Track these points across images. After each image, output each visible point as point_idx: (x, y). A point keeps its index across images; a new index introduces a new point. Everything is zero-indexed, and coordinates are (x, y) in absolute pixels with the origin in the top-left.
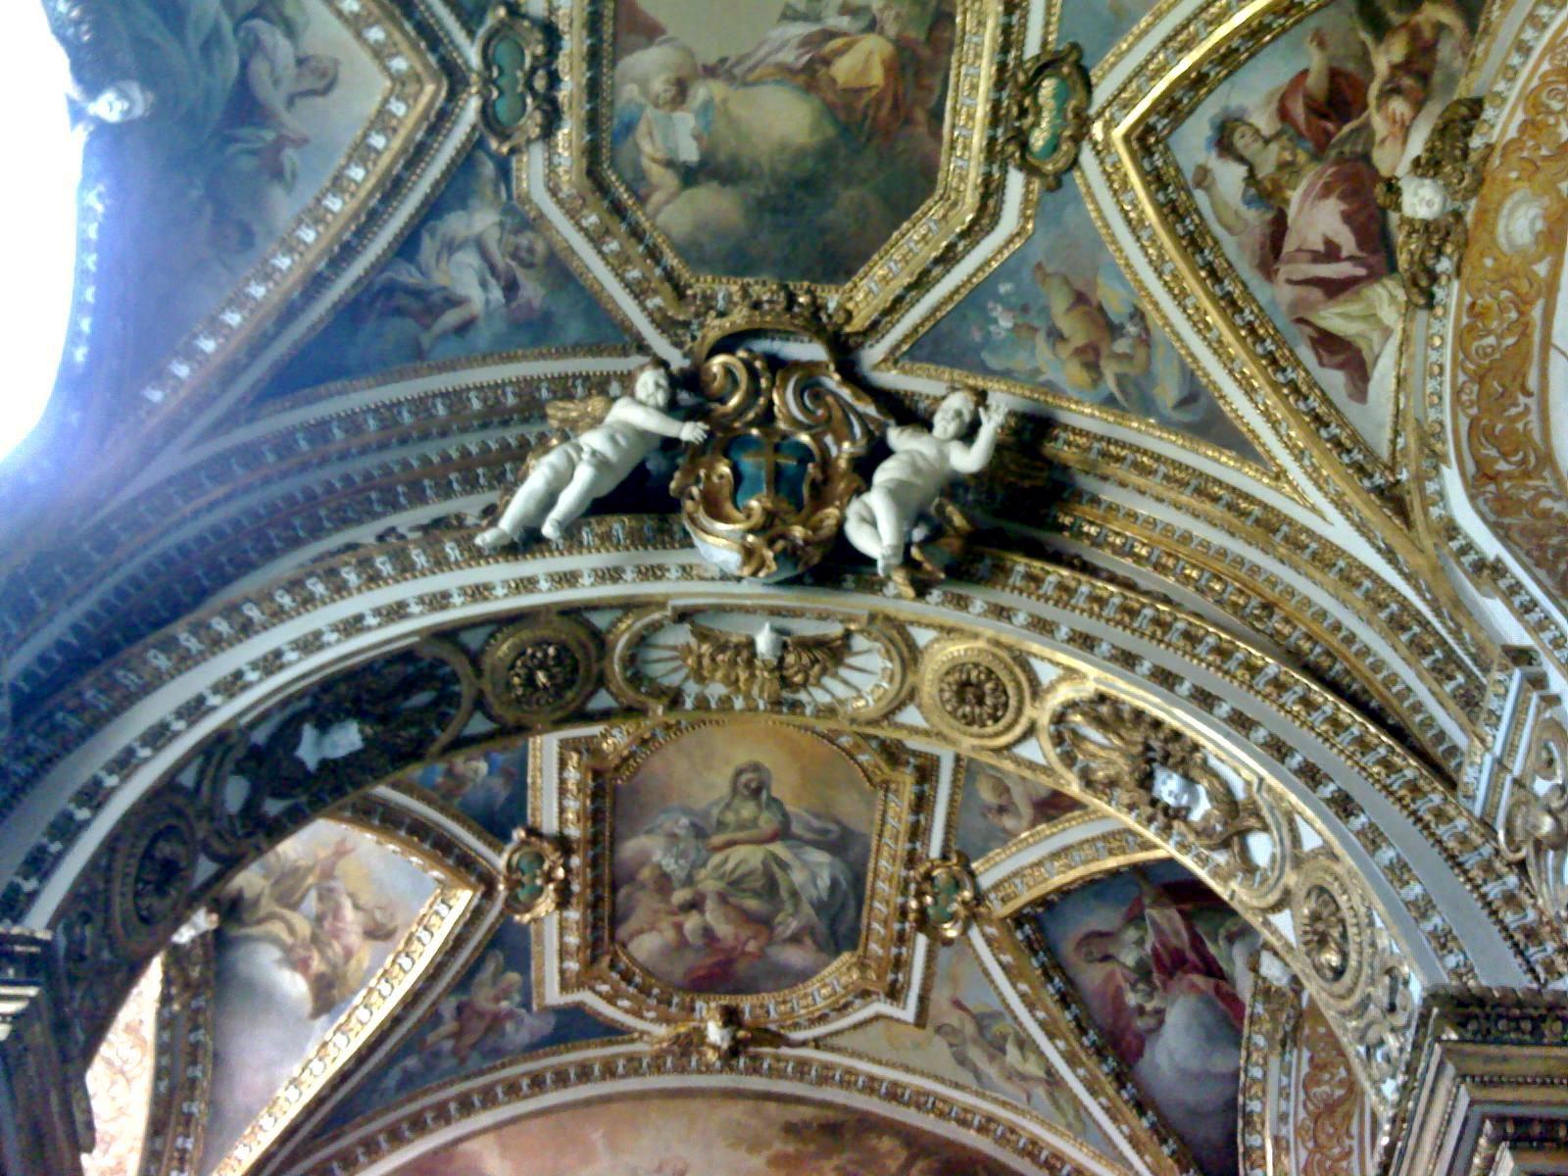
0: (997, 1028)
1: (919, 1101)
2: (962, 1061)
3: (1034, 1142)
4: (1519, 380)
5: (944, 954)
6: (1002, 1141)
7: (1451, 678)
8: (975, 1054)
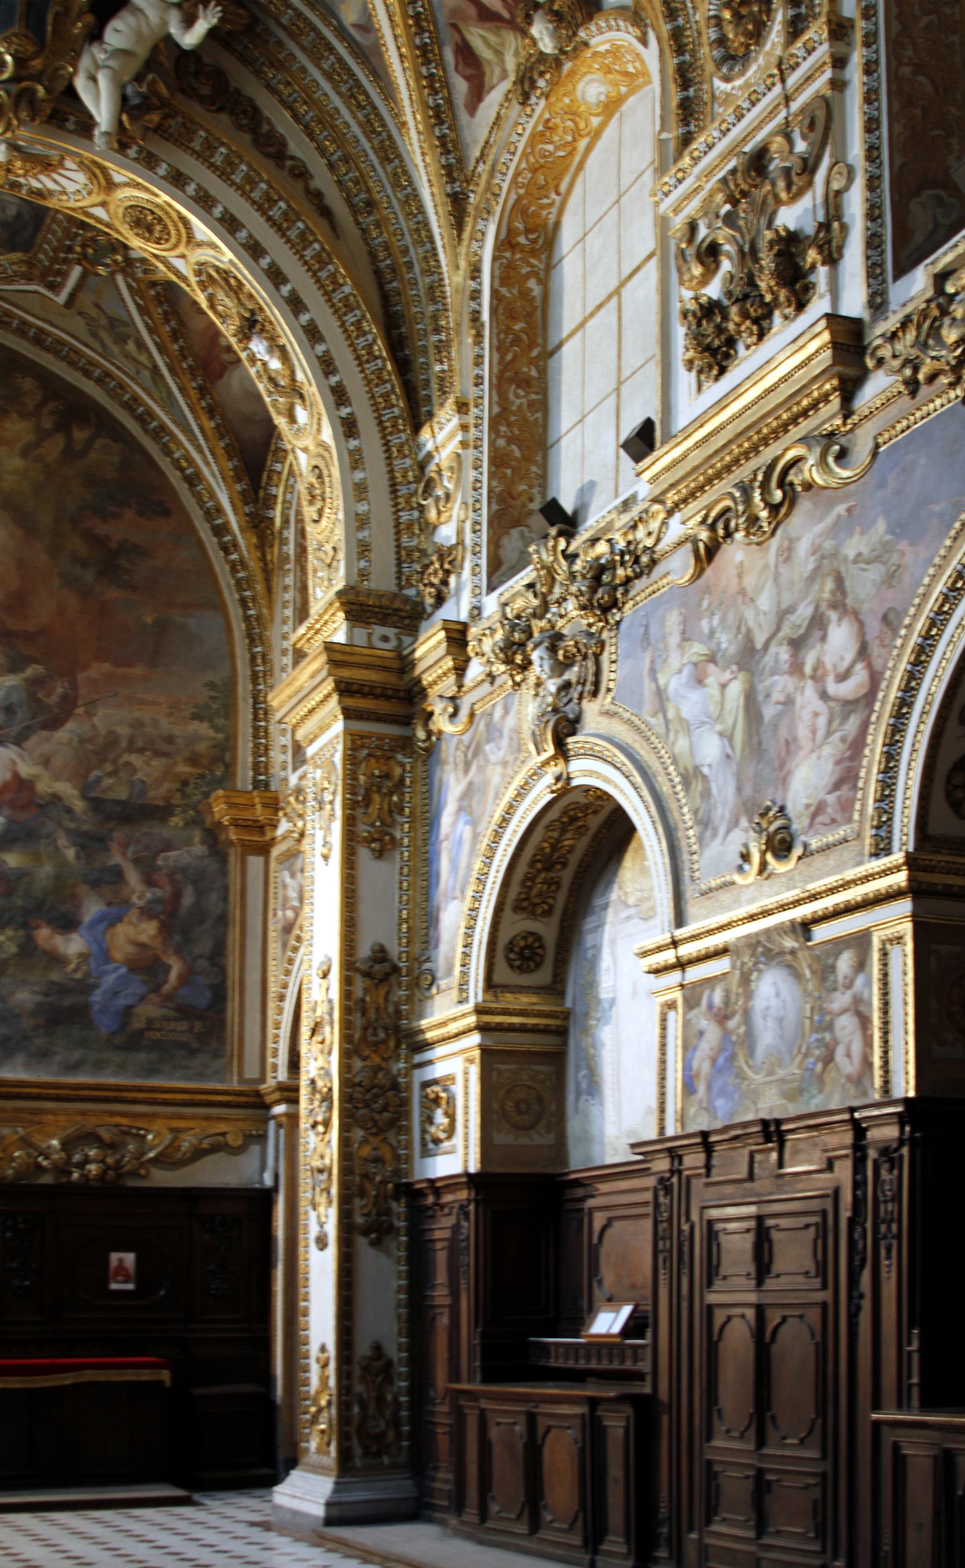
0: (123, 329)
1: (58, 349)
2: (94, 335)
3: (136, 399)
4: (555, 182)
5: (92, 280)
6: (112, 394)
7: (441, 362)
8: (103, 334)
